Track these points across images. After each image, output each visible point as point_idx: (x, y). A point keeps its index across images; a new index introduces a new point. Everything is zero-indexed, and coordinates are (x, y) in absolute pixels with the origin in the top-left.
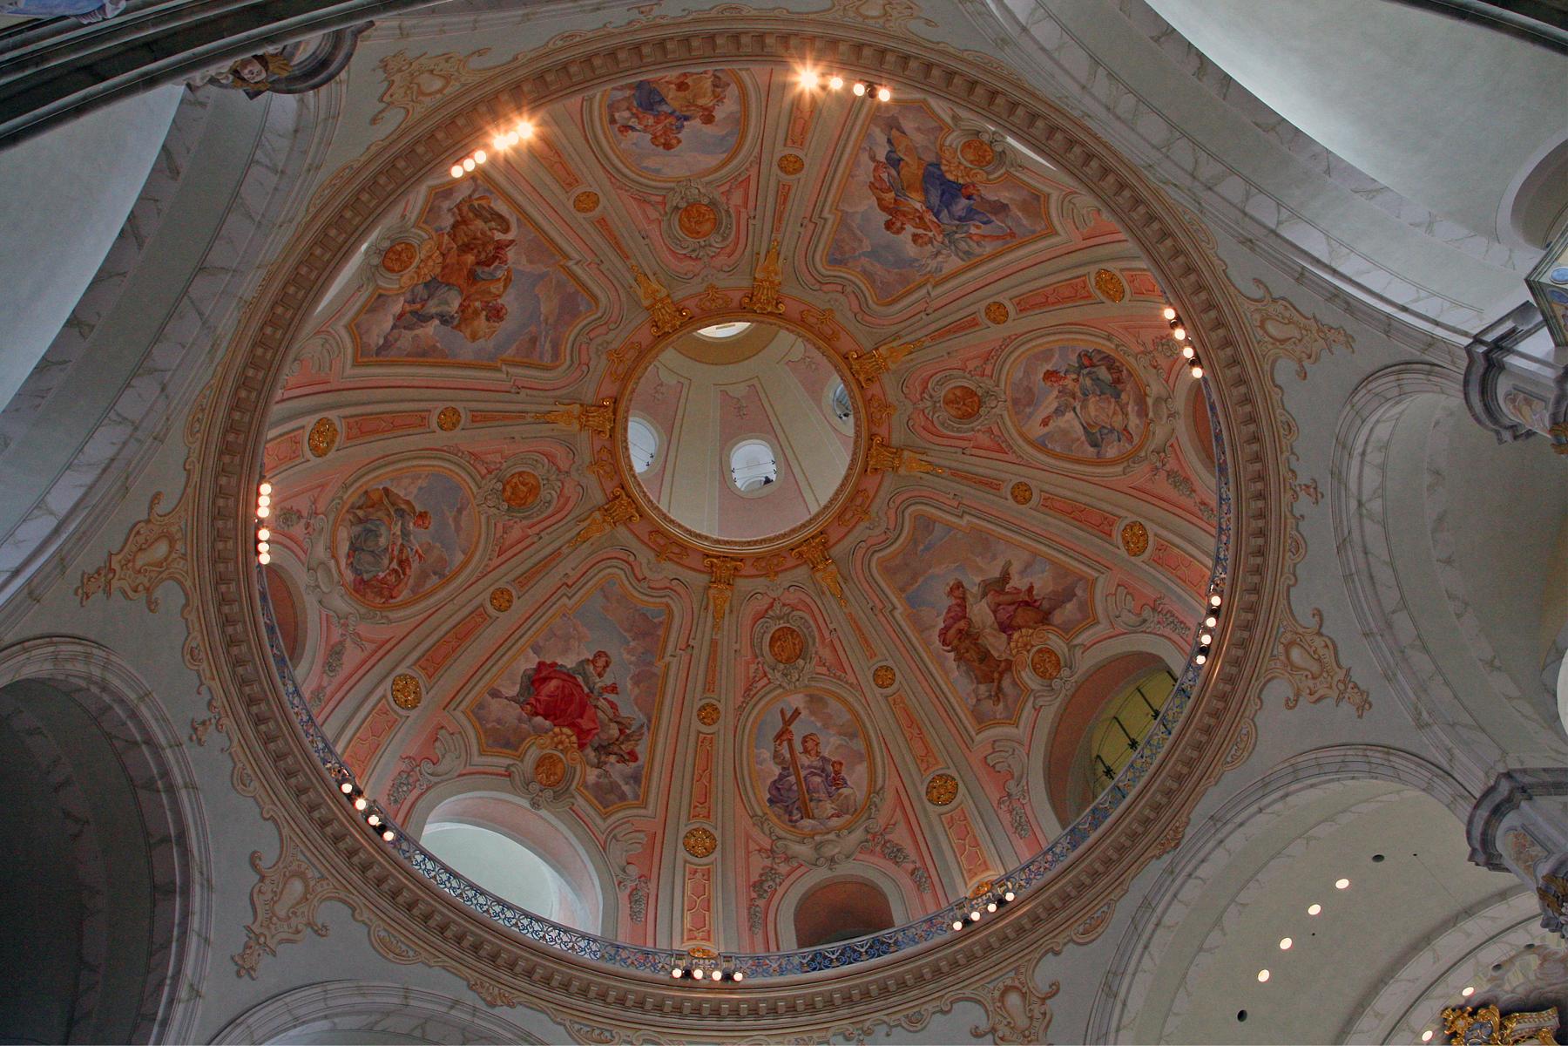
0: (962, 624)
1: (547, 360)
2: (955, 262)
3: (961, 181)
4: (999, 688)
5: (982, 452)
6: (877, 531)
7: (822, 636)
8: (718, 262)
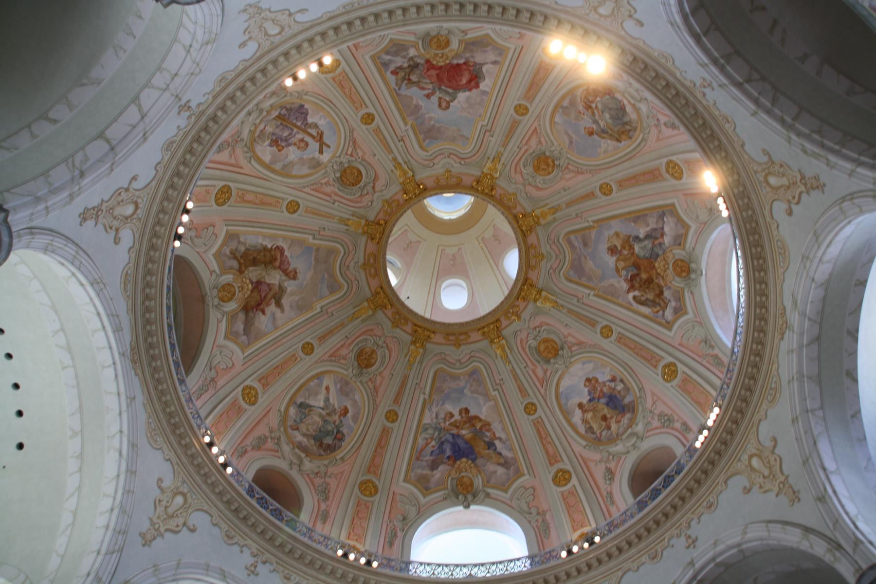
0: (277, 263)
1: (572, 237)
2: (427, 420)
3: (458, 462)
4: (235, 258)
5: (339, 345)
6: (352, 265)
7: (336, 194)
8: (523, 335)
